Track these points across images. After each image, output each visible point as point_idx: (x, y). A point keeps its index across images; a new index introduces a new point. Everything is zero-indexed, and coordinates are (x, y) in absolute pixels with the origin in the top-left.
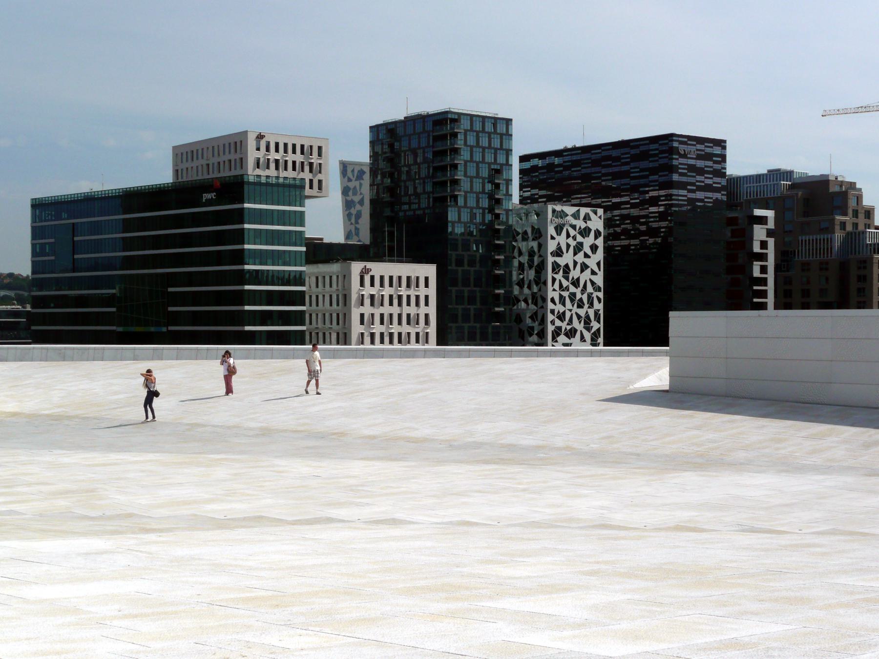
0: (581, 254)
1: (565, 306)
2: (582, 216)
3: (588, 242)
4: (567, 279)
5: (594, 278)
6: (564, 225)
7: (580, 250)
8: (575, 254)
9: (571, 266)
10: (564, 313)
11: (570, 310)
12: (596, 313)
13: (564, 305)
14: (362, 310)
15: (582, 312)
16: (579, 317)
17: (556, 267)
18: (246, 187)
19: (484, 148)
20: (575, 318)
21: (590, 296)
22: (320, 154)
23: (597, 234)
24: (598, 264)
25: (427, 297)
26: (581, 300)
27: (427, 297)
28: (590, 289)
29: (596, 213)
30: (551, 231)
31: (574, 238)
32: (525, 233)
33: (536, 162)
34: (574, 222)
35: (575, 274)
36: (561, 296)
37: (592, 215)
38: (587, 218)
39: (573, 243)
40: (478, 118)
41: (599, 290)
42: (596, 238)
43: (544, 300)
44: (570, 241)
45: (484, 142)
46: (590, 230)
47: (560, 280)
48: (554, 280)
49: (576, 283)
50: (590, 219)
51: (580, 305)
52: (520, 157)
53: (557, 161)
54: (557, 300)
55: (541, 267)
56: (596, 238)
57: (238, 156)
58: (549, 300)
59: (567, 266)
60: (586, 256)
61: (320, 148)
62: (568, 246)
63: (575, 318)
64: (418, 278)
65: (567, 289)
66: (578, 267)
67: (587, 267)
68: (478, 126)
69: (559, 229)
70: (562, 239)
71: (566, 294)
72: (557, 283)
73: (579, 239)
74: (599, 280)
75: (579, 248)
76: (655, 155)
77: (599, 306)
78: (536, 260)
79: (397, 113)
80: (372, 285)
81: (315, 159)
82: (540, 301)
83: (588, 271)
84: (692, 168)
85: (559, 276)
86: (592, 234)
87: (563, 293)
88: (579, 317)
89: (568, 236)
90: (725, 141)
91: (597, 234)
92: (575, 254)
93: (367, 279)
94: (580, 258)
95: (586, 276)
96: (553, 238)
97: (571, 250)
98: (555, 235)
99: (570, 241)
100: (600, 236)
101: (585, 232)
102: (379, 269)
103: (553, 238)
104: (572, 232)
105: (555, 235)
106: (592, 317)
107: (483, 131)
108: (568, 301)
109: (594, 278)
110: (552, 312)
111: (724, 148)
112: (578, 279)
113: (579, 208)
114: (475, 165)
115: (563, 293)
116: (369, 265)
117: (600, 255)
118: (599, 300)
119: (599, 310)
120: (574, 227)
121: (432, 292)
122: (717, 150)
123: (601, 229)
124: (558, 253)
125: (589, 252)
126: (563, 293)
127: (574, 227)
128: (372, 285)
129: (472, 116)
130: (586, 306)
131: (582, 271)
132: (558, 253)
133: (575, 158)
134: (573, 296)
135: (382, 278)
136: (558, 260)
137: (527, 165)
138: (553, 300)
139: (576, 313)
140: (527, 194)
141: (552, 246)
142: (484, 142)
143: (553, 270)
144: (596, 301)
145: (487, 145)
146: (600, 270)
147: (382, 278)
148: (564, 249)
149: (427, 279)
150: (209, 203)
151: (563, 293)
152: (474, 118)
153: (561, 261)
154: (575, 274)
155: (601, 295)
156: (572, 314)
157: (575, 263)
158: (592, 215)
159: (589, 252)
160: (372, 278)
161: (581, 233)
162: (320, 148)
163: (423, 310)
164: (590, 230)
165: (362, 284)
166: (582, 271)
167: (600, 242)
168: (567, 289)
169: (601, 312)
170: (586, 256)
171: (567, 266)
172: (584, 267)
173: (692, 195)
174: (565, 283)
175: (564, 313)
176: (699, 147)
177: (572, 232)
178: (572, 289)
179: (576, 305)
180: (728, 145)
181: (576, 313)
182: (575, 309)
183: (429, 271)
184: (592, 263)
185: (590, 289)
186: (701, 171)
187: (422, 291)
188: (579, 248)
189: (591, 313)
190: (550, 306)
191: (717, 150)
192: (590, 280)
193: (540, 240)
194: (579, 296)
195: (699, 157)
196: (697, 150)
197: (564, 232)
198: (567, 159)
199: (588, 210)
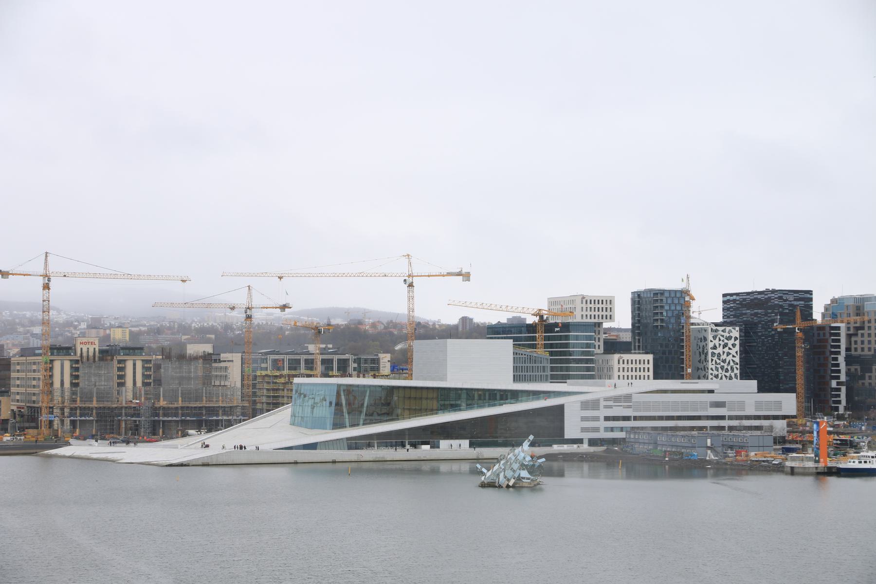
0: (727, 348)
1: (718, 372)
2: (727, 331)
3: (730, 343)
4: (720, 360)
5: (734, 359)
6: (717, 335)
7: (726, 346)
8: (723, 348)
9: (722, 354)
10: (718, 375)
11: (721, 374)
12: (736, 375)
13: (718, 371)
14: (619, 374)
15: (728, 374)
16: (726, 376)
17: (713, 354)
18: (570, 327)
19: (676, 304)
20: (724, 377)
21: (732, 368)
22: (610, 303)
23: (736, 339)
24: (737, 352)
25: (648, 368)
26: (727, 369)
27: (648, 368)
28: (732, 364)
29: (735, 329)
30: (710, 338)
31: (723, 341)
32: (701, 338)
33: (728, 297)
34: (723, 334)
35: (723, 357)
36: (716, 367)
37: (732, 330)
38: (730, 331)
39: (722, 343)
40: (673, 292)
41: (737, 364)
42: (735, 340)
43: (708, 369)
44: (721, 342)
46: (732, 337)
47: (716, 360)
48: (712, 360)
49: (724, 361)
50: (731, 332)
51: (727, 371)
52: (723, 295)
53: (738, 298)
54: (714, 369)
55: (707, 354)
56: (735, 340)
57: (574, 306)
58: (710, 369)
59: (719, 353)
60: (730, 349)
61: (610, 301)
62: (720, 345)
63: (724, 377)
64: (644, 360)
65: (719, 364)
66: (725, 354)
67: (730, 354)
68: (673, 295)
69: (715, 337)
70: (717, 342)
71: (719, 366)
72: (714, 362)
73: (726, 341)
74: (737, 360)
75: (725, 346)
76: (773, 299)
77: (738, 372)
78: (705, 351)
79: (641, 287)
80: (623, 363)
81: (609, 306)
82: (706, 370)
83: (731, 356)
85: (715, 358)
86: (733, 339)
87: (718, 366)
88: (726, 376)
89: (720, 340)
90: (812, 291)
91: (736, 339)
92: (723, 348)
94: (726, 350)
95: (730, 357)
96: (711, 341)
97: (722, 346)
98: (713, 340)
99: (721, 342)
100: (737, 339)
101: (729, 338)
102: (626, 357)
103: (711, 341)
104: (722, 338)
105: (713, 340)
106: (733, 376)
107: (676, 297)
108: (720, 369)
109: (734, 359)
110: (712, 374)
111: (812, 294)
112: (725, 359)
113: (725, 328)
114: (671, 312)
115: (717, 366)
116: (622, 355)
117: (737, 348)
118: (737, 369)
119: (737, 373)
120: (723, 336)
121: (651, 366)
122: (808, 296)
123: (738, 337)
124: (715, 347)
125: (731, 347)
126: (718, 366)
127: (723, 336)
128: (623, 363)
129: (670, 291)
130: (730, 371)
131: (727, 356)
132: (715, 347)
133: (744, 297)
134: (722, 368)
135: (628, 360)
136: (714, 351)
137: (726, 299)
138: (712, 369)
139: (725, 375)
140: (725, 314)
141: (711, 345)
142: (676, 301)
143: (712, 356)
144: (735, 369)
145: (677, 302)
146: (737, 355)
147: (628, 360)
148: (718, 346)
149: (648, 361)
150: (557, 332)
151: (717, 366)
152: (671, 292)
153: (716, 351)
155: (738, 366)
156: (722, 376)
157: (724, 352)
158: (733, 330)
159: (731, 347)
160: (623, 361)
162: (610, 301)
163: (646, 374)
164: (732, 337)
165: (619, 363)
166: (727, 356)
167: (737, 342)
168: (719, 364)
169: (738, 375)
170: (730, 349)
171: (719, 353)
172: (729, 354)
174: (718, 361)
175: (718, 375)
176: (795, 295)
177: (722, 338)
178: (722, 364)
179: (724, 371)
180: (814, 293)
181: (725, 375)
182: (724, 373)
183: (650, 357)
184: (733, 352)
185: (732, 364)
187: (646, 366)
188: (725, 346)
189: (733, 376)
190: (710, 371)
191: (808, 296)
192: (732, 360)
193: (706, 342)
194: (726, 367)
195: (795, 300)
196: (794, 297)
197: (718, 339)
198: (741, 297)
199: (730, 328)
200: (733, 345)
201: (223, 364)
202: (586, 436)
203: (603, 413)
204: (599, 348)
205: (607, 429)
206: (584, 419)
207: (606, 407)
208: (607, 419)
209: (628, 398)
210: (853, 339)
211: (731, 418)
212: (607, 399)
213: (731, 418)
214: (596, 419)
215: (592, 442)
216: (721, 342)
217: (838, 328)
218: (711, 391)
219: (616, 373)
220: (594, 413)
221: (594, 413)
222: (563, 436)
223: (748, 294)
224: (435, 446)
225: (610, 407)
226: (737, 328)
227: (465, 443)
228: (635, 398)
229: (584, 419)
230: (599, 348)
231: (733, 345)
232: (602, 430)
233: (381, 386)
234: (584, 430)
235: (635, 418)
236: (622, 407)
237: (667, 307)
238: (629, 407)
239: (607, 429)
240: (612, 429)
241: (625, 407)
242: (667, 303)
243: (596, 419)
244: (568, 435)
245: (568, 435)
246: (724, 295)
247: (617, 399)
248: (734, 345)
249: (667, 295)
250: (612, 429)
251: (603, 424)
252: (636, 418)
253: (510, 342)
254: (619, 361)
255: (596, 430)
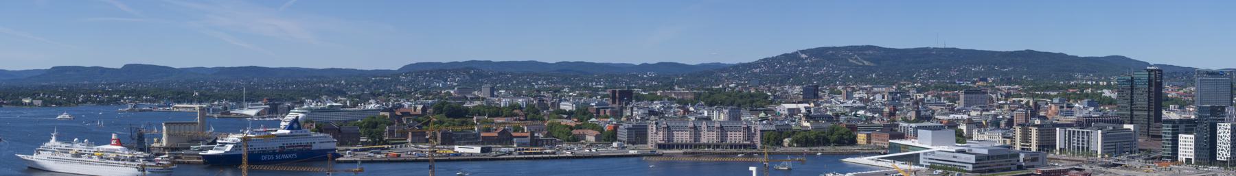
3: (1227, 130)
35: (1223, 138)
69: (1220, 128)
70: (1221, 131)
74: (1229, 139)
75: (1224, 132)
77: (1229, 145)
94: (1225, 134)
95: (1226, 138)
101: (1226, 129)
124: (1220, 133)
132: (1220, 133)
154: (1223, 138)
167: (1230, 131)
188: (1224, 132)
206: (924, 158)
208: (929, 159)
211: (959, 162)
213: (959, 162)
214: (926, 159)
243: (926, 159)
245: (921, 163)
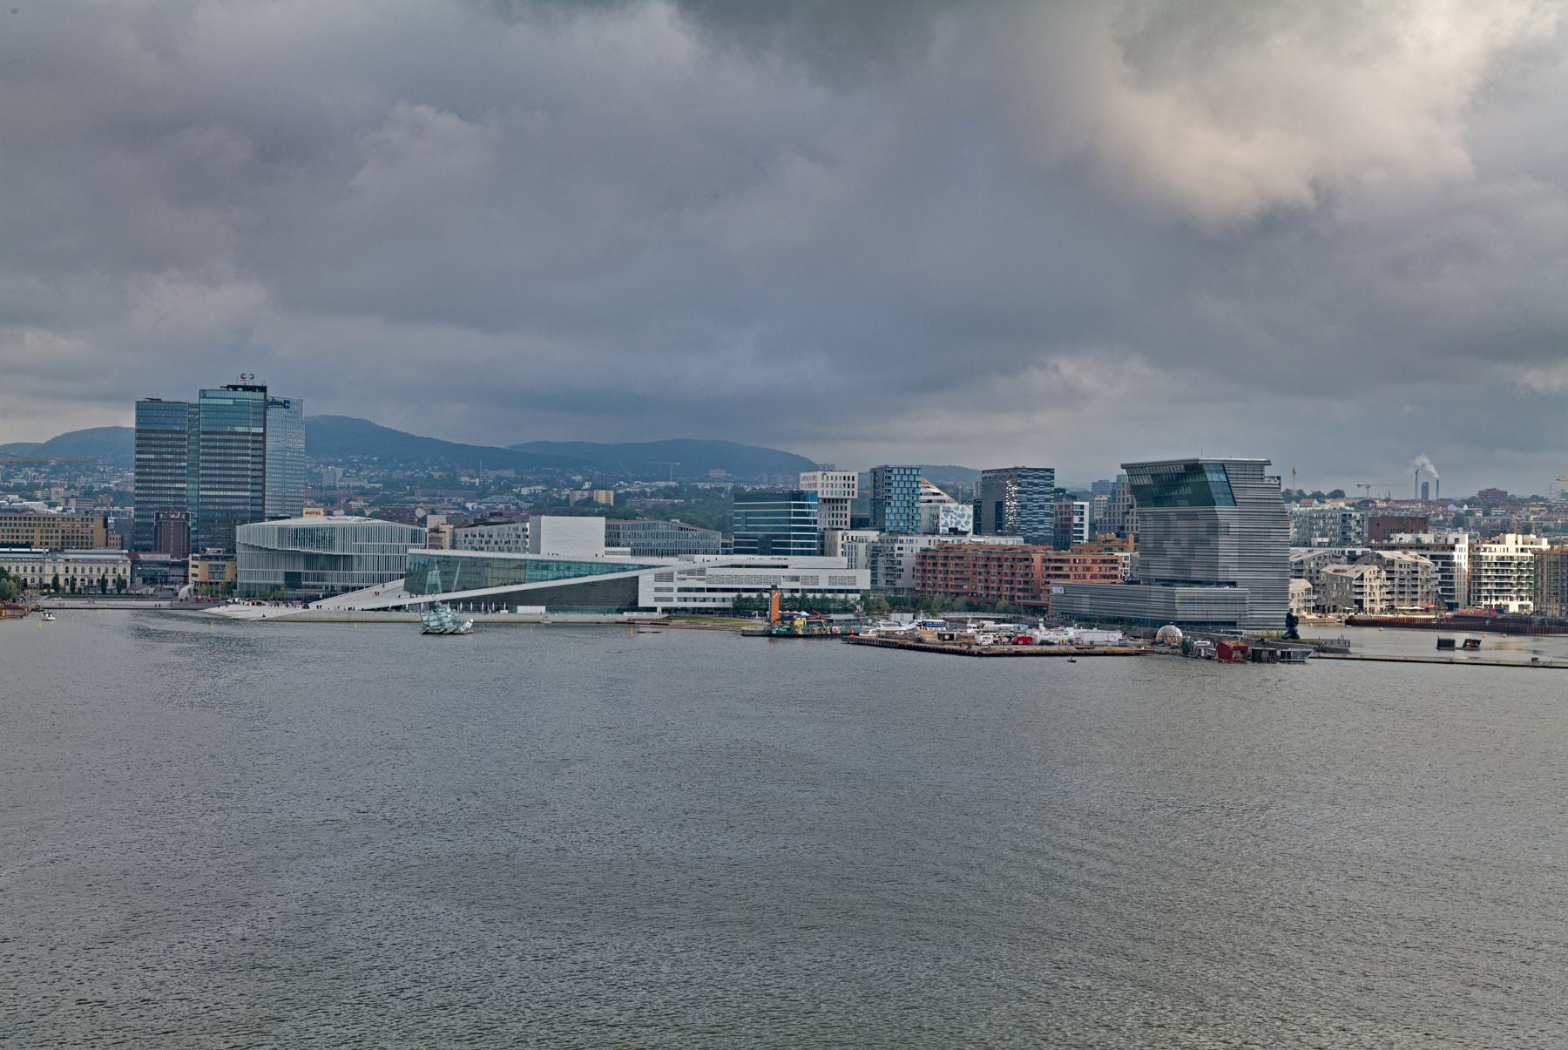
31: (955, 519)
42: (968, 518)
45: (905, 478)
56: (968, 518)
68: (902, 472)
73: (958, 519)
84: (1029, 483)
86: (966, 517)
89: (952, 517)
93: (845, 537)
99: (953, 520)
101: (962, 516)
104: (954, 516)
137: (984, 475)
158: (967, 508)
161: (960, 516)
167: (971, 520)
173: (1029, 497)
177: (954, 516)
186: (1037, 485)
200: (966, 523)
201: (440, 535)
202: (660, 605)
203: (676, 584)
204: (846, 524)
205: (679, 599)
206: (657, 590)
207: (679, 579)
208: (680, 590)
209: (702, 571)
210: (1127, 517)
212: (679, 573)
214: (671, 590)
215: (664, 610)
216: (953, 520)
217: (1082, 507)
218: (786, 567)
219: (840, 550)
220: (669, 585)
221: (669, 585)
222: (637, 604)
223: (999, 471)
224: (512, 610)
225: (684, 579)
226: (971, 506)
227: (543, 609)
228: (709, 572)
229: (657, 590)
230: (846, 524)
231: (966, 523)
232: (675, 600)
233: (471, 558)
234: (657, 599)
235: (710, 590)
236: (694, 580)
237: (895, 484)
238: (704, 579)
239: (679, 599)
240: (685, 600)
241: (699, 579)
242: (895, 480)
243: (671, 590)
244: (639, 606)
246: (983, 472)
247: (690, 572)
248: (967, 523)
249: (895, 472)
250: (685, 600)
251: (675, 594)
252: (710, 590)
253: (604, 518)
254: (843, 537)
255: (670, 600)
